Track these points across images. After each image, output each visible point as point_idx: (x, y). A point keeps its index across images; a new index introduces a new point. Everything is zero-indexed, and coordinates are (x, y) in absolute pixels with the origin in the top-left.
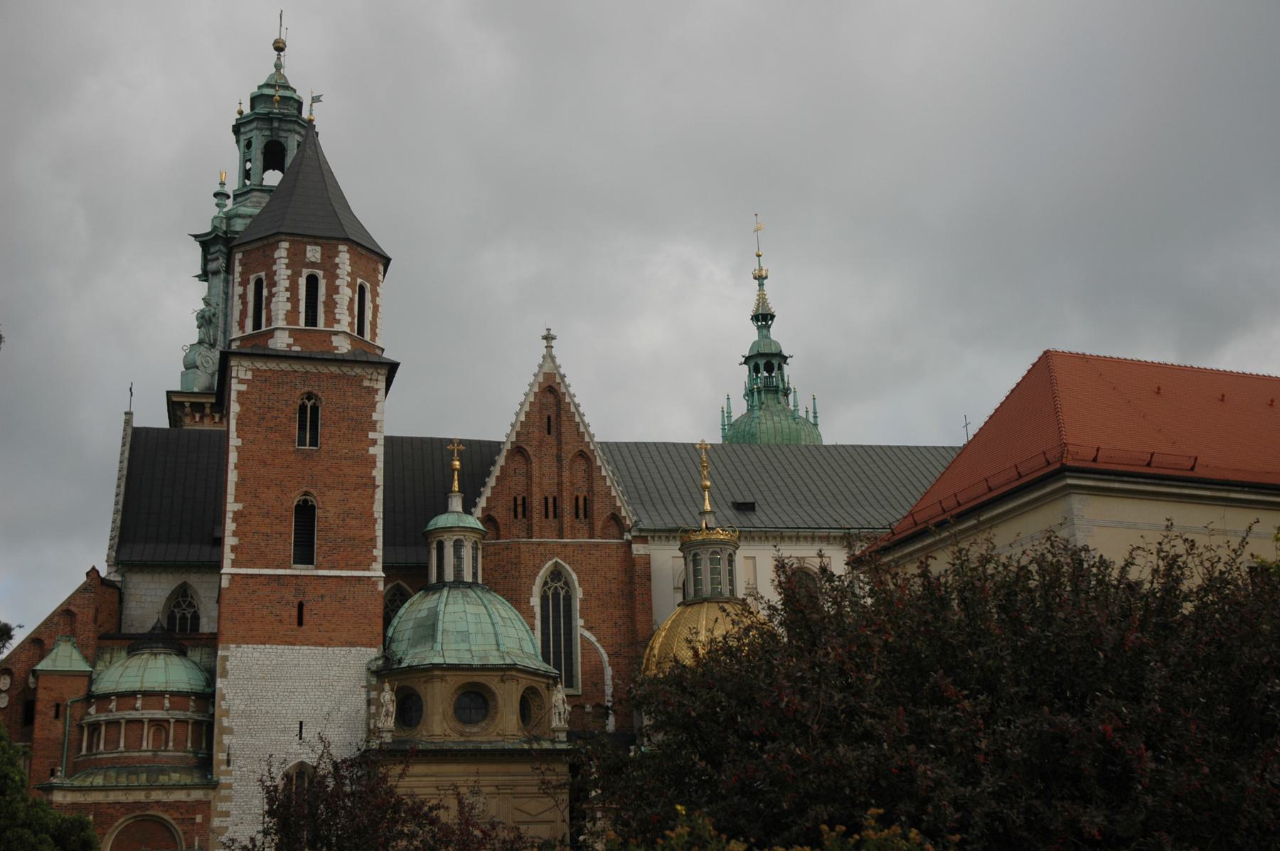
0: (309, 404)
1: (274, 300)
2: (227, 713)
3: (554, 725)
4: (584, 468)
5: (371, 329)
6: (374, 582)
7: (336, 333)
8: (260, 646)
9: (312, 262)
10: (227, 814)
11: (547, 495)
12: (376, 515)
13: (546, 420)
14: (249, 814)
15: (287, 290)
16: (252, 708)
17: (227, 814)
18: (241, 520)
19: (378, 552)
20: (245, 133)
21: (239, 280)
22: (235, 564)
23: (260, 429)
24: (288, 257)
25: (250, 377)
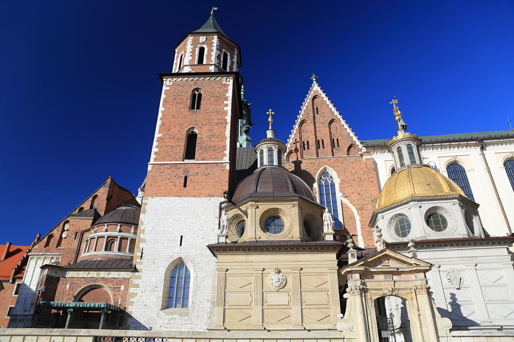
0: (197, 93)
1: (185, 57)
3: (325, 231)
4: (336, 127)
5: (230, 69)
7: (212, 65)
10: (138, 286)
11: (319, 139)
12: (226, 136)
13: (315, 109)
15: (191, 53)
16: (156, 229)
17: (138, 286)
18: (161, 141)
19: (227, 152)
22: (155, 159)
23: (173, 103)
24: (192, 42)
25: (171, 84)
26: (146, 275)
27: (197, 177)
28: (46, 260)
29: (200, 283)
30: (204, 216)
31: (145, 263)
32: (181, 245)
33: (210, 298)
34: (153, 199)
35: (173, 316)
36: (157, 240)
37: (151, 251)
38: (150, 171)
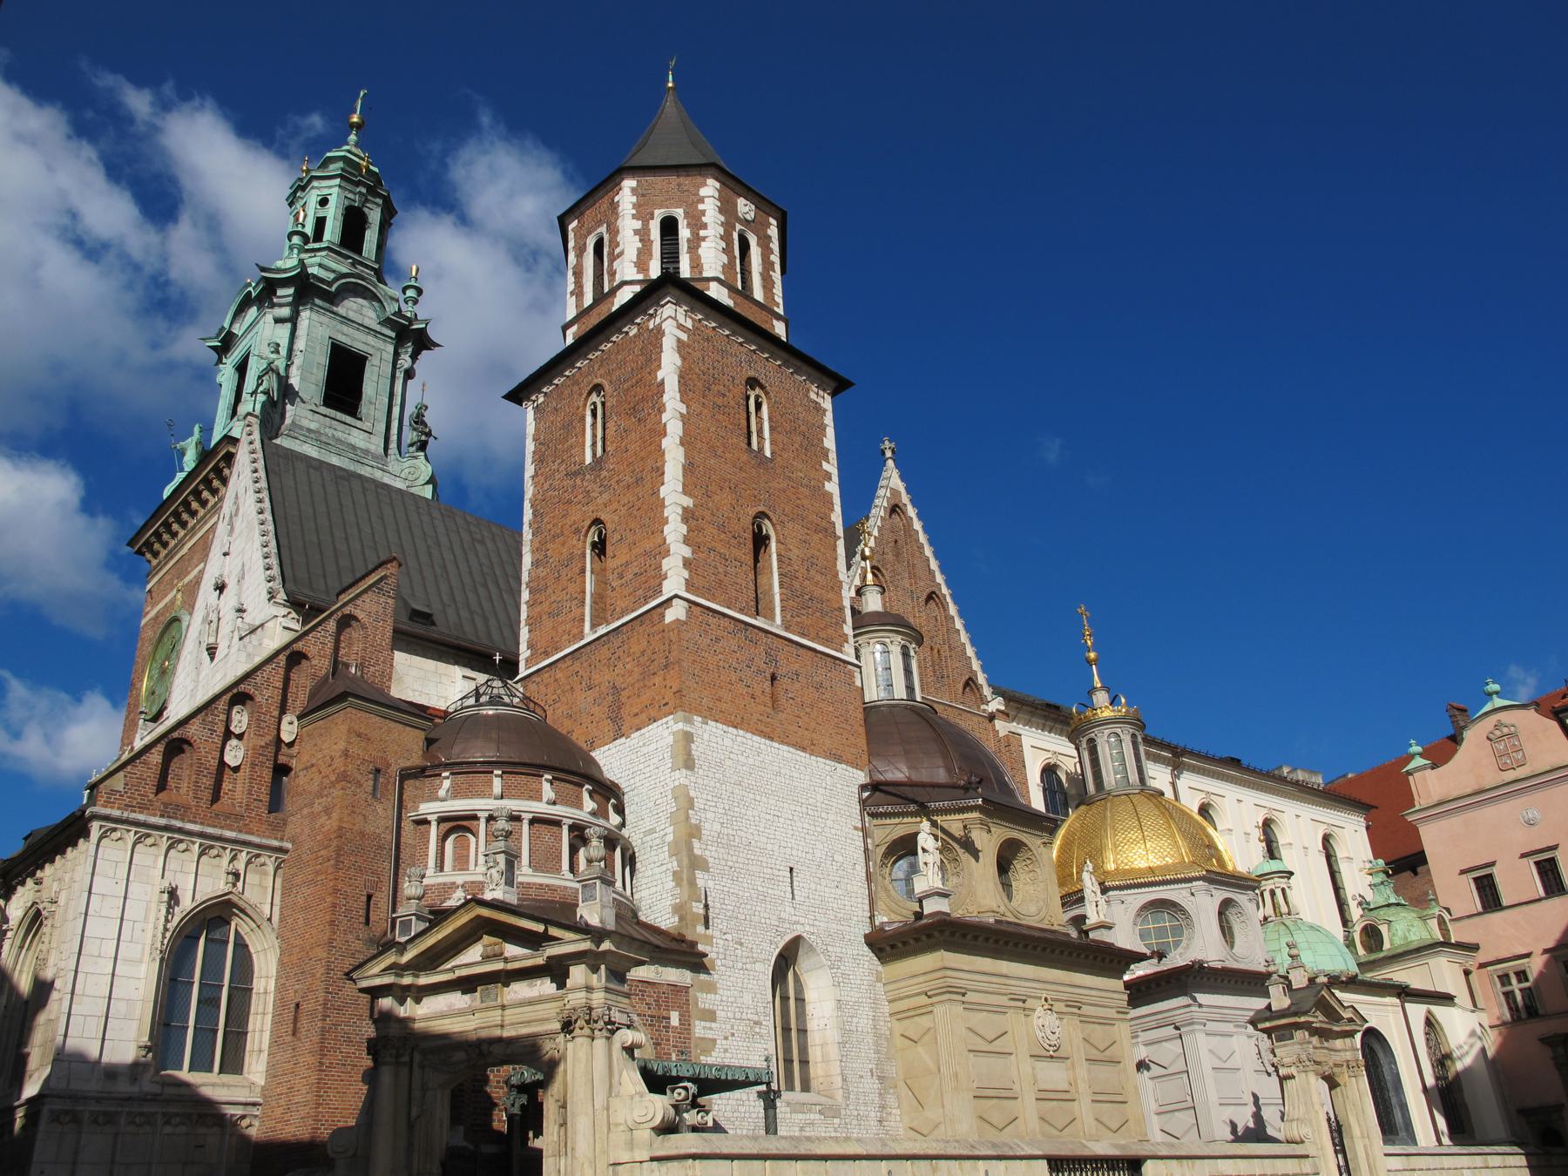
1: (703, 244)
2: (695, 832)
6: (850, 671)
7: (778, 317)
8: (731, 729)
9: (746, 220)
10: (710, 1016)
14: (741, 1019)
16: (730, 832)
17: (710, 1016)
20: (318, 188)
21: (634, 212)
24: (719, 200)
26: (729, 983)
27: (797, 685)
28: (172, 852)
29: (849, 1019)
30: (831, 817)
31: (719, 941)
32: (793, 898)
33: (874, 1066)
34: (707, 727)
35: (808, 1116)
36: (738, 870)
37: (726, 902)
38: (685, 623)
